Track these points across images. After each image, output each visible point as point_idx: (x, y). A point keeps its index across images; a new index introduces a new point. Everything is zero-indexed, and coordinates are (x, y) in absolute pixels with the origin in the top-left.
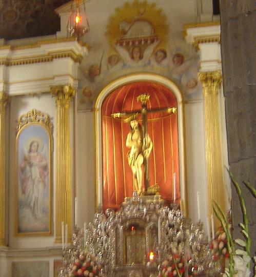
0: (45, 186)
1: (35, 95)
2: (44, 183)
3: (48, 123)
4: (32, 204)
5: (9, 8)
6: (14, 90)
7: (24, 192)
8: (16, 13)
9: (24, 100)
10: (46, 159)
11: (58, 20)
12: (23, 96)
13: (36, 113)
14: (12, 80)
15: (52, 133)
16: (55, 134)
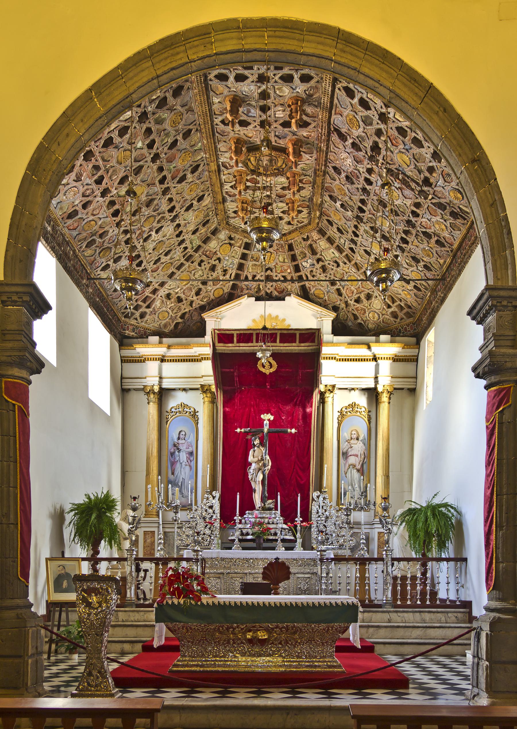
0: (191, 469)
1: (184, 390)
2: (190, 466)
3: (194, 415)
4: (180, 484)
5: (164, 309)
6: (166, 384)
7: (173, 473)
8: (168, 313)
9: (173, 393)
10: (192, 446)
11: (203, 323)
12: (174, 389)
13: (184, 406)
14: (164, 375)
15: (198, 423)
16: (200, 426)
